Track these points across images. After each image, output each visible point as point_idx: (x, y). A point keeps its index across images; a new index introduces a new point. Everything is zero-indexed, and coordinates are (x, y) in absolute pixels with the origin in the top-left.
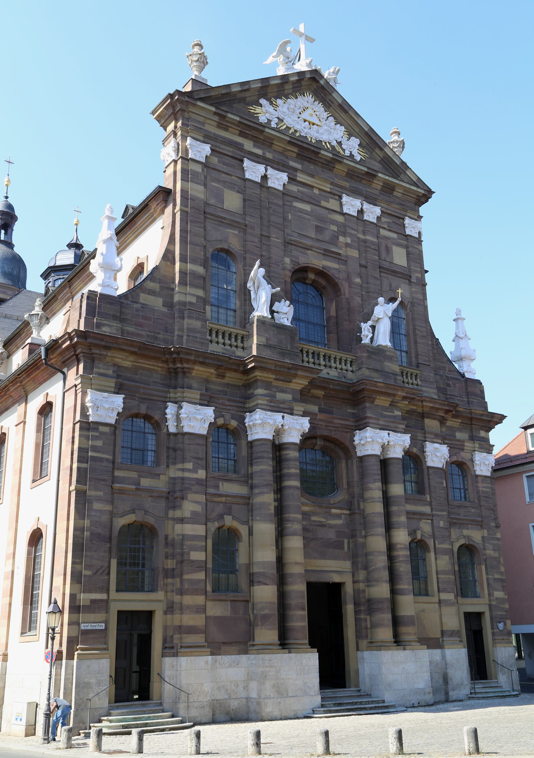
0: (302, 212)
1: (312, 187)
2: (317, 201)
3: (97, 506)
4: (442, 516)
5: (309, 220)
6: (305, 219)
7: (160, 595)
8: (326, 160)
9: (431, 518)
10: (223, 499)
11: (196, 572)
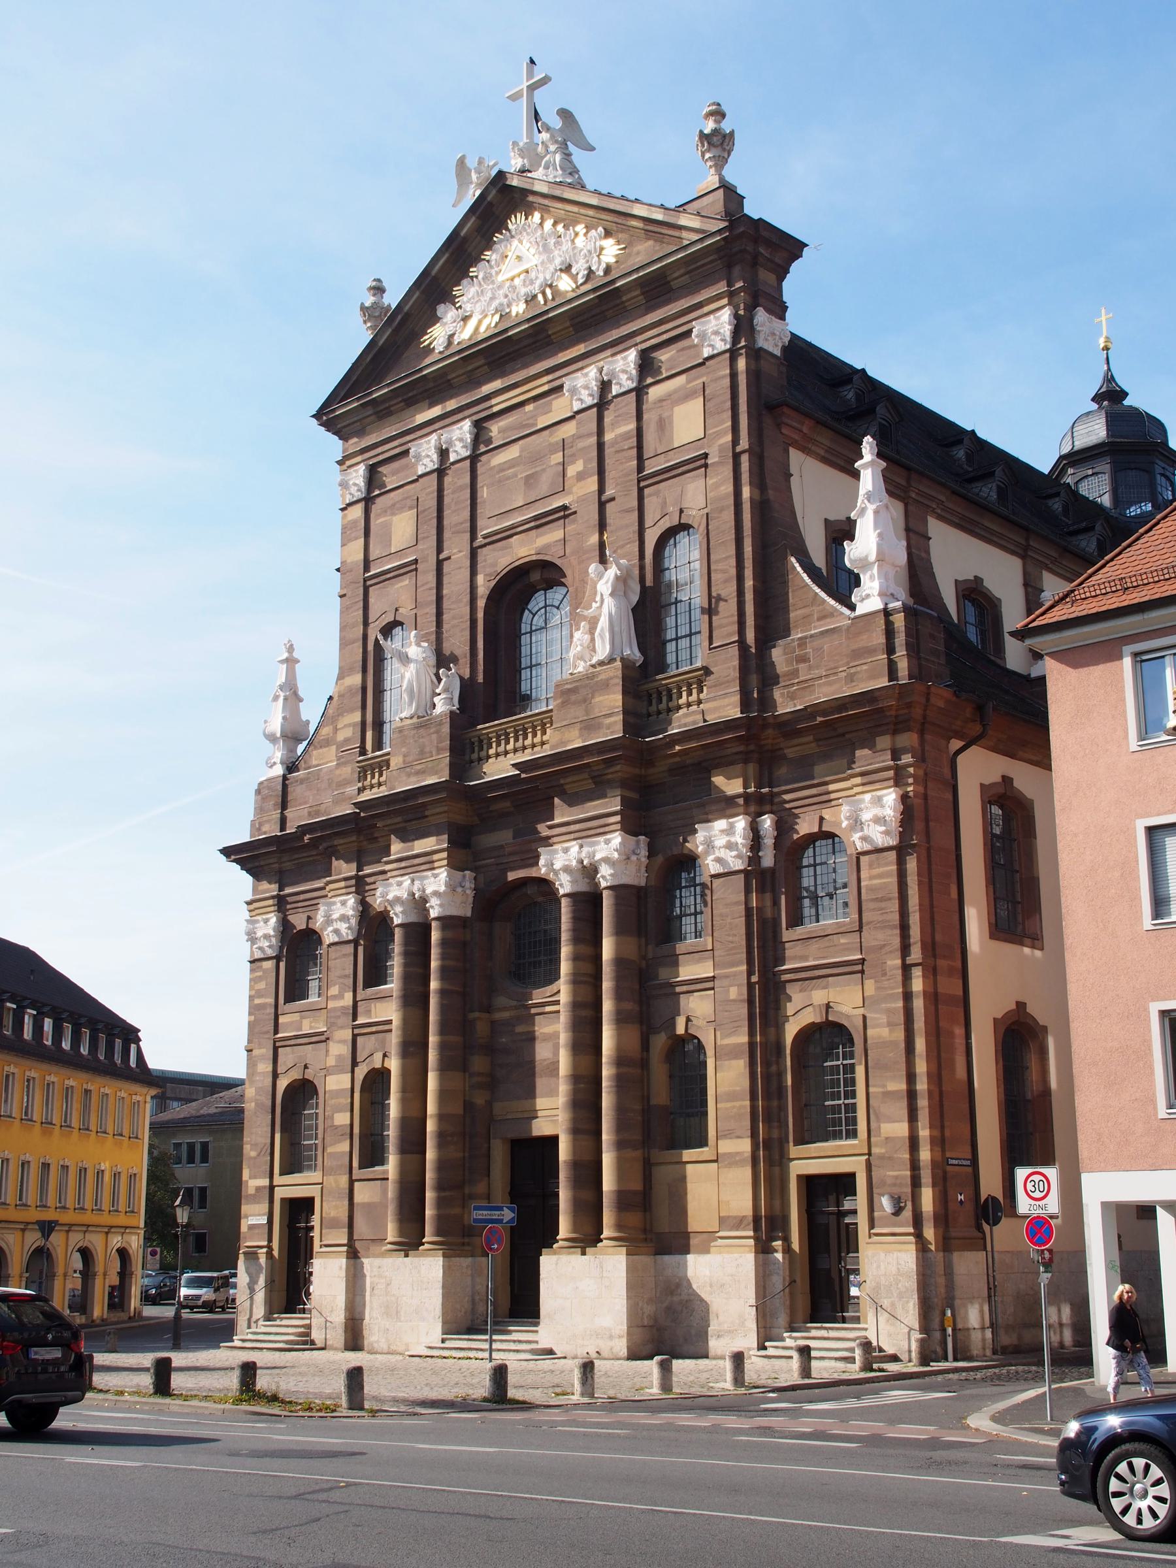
1: (522, 404)
4: (735, 974)
6: (508, 478)
8: (529, 336)
9: (710, 985)
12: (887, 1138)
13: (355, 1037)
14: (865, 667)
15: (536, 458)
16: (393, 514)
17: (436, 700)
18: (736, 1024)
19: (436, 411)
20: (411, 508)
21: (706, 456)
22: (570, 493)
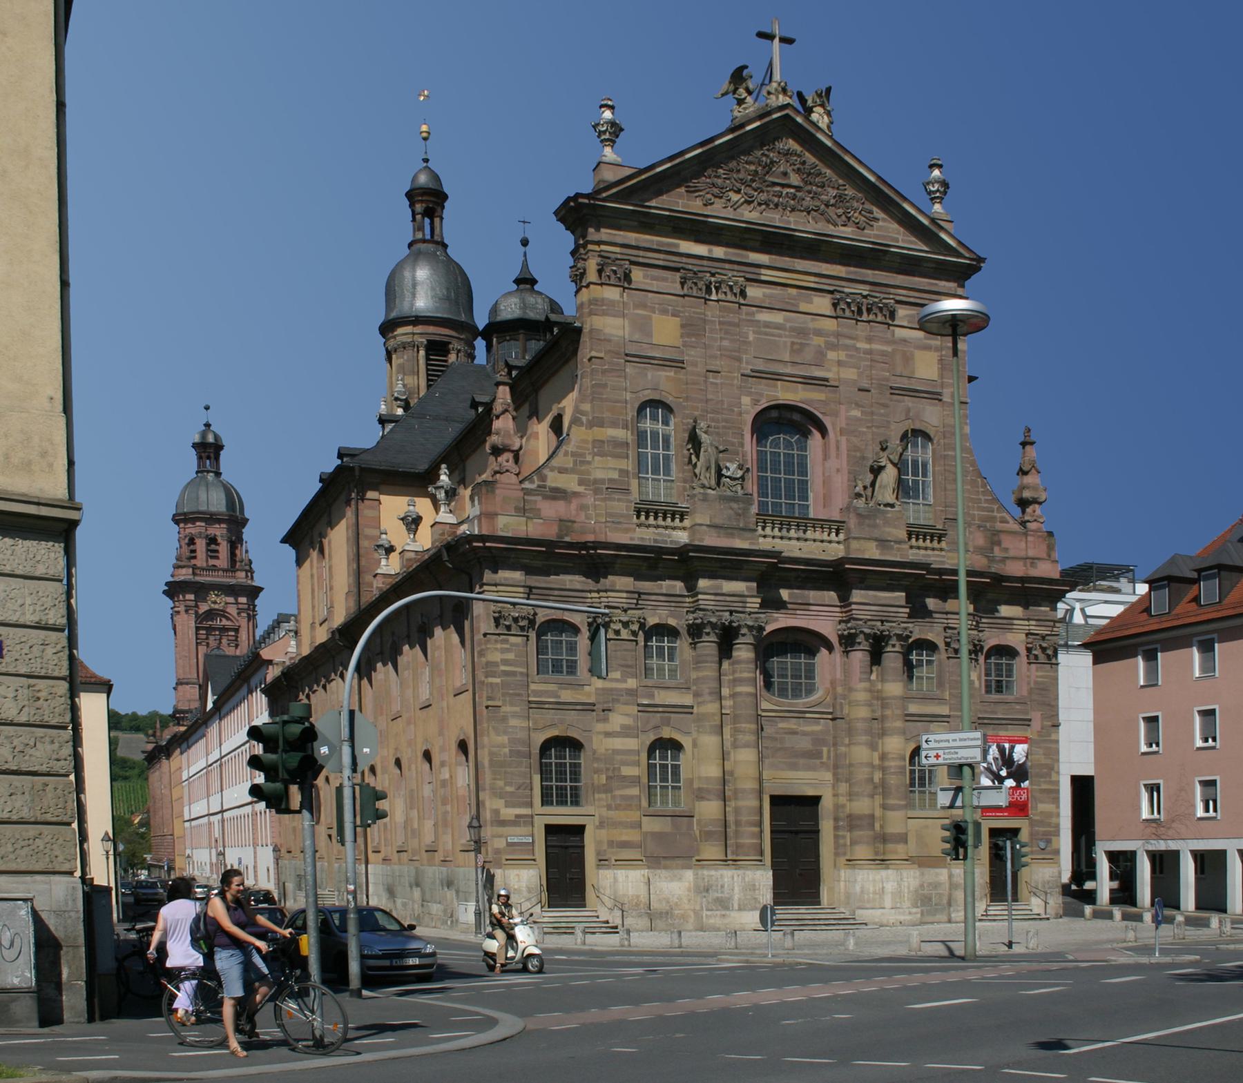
2: (793, 305)
3: (513, 722)
11: (627, 787)
15: (802, 332)
22: (829, 370)
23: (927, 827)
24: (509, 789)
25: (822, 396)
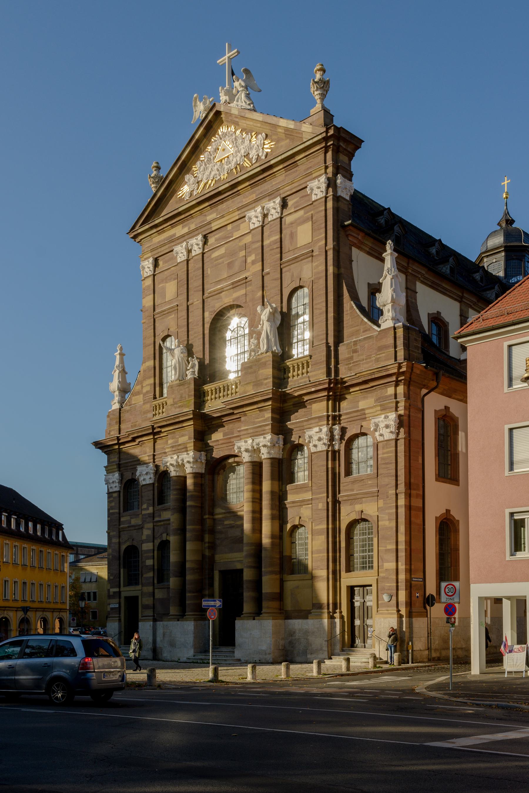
0: (217, 260)
4: (321, 498)
5: (223, 262)
6: (220, 264)
7: (139, 587)
10: (162, 523)
12: (386, 569)
13: (154, 526)
14: (384, 355)
16: (166, 282)
17: (187, 372)
18: (321, 520)
19: (186, 230)
20: (174, 279)
21: (313, 251)
22: (249, 271)
23: (298, 587)
24: (112, 578)
25: (243, 292)
